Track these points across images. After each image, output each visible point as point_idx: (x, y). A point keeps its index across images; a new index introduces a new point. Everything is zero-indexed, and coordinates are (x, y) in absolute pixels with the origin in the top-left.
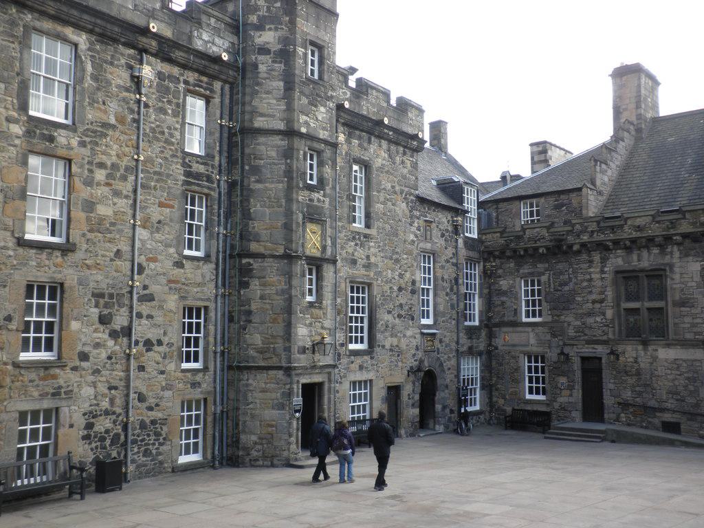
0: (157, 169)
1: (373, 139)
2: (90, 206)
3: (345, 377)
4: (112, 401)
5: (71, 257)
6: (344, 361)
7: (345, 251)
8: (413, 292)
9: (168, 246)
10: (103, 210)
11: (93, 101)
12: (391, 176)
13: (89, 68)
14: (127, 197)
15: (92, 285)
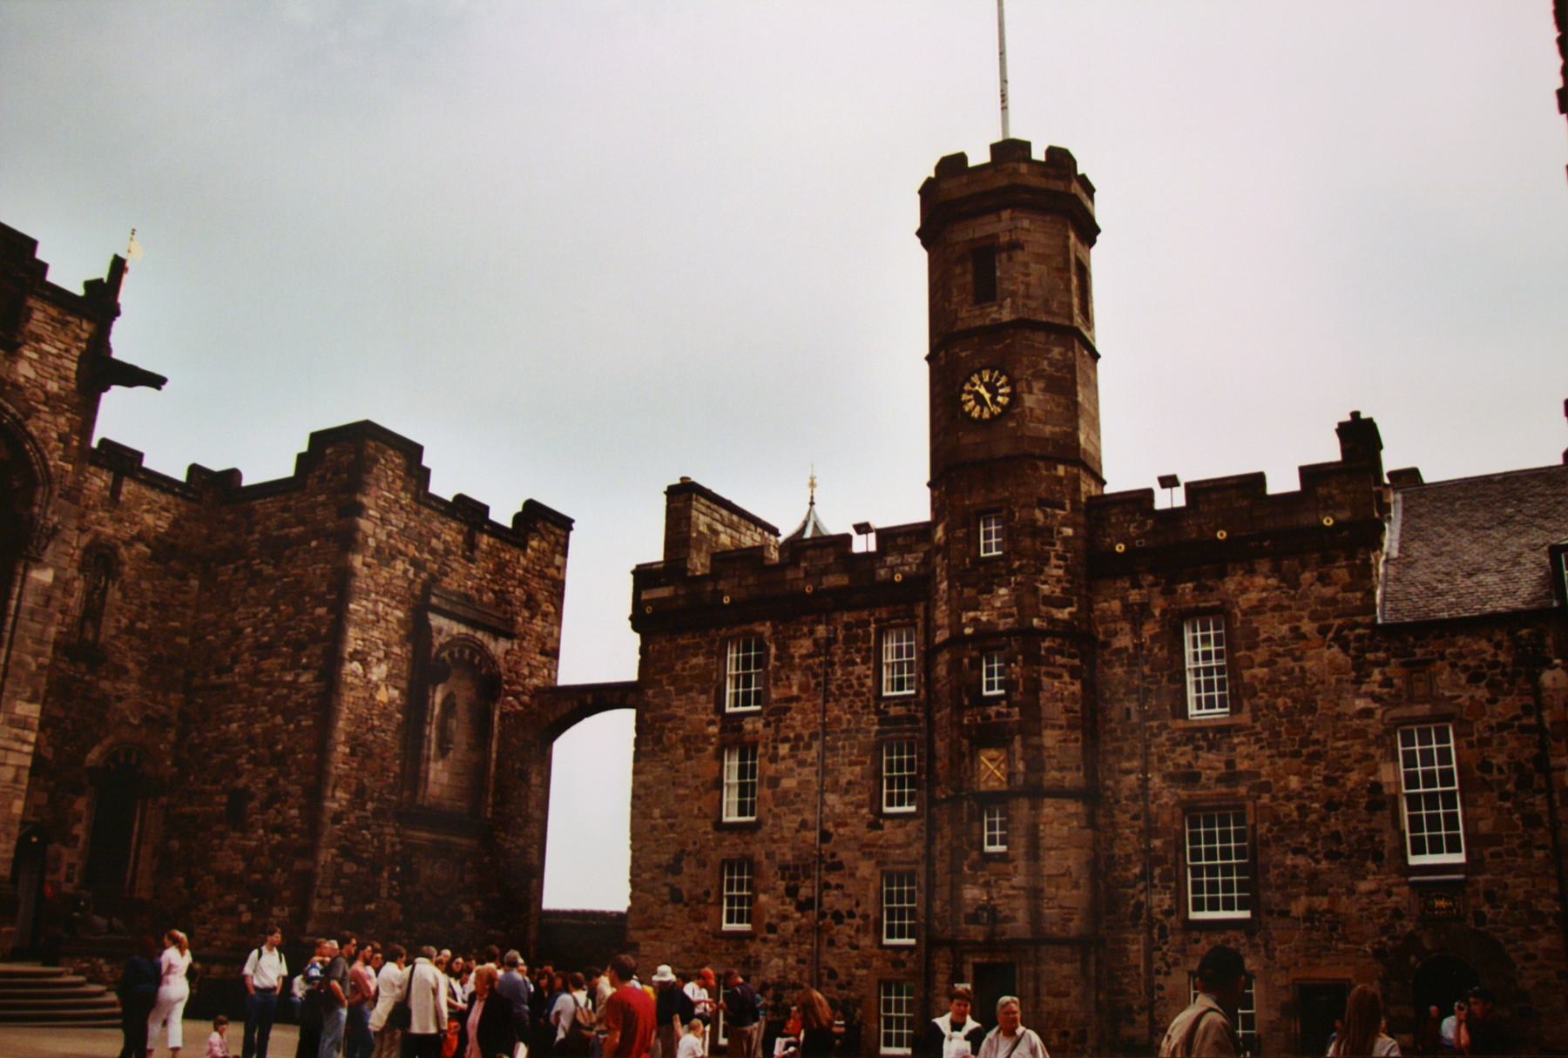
0: (844, 726)
1: (1230, 567)
2: (774, 782)
3: (1176, 963)
4: (800, 973)
5: (760, 834)
6: (1175, 940)
7: (1170, 763)
8: (1373, 807)
9: (860, 806)
10: (788, 783)
11: (777, 679)
12: (1286, 614)
13: (773, 650)
14: (812, 765)
15: (778, 857)
